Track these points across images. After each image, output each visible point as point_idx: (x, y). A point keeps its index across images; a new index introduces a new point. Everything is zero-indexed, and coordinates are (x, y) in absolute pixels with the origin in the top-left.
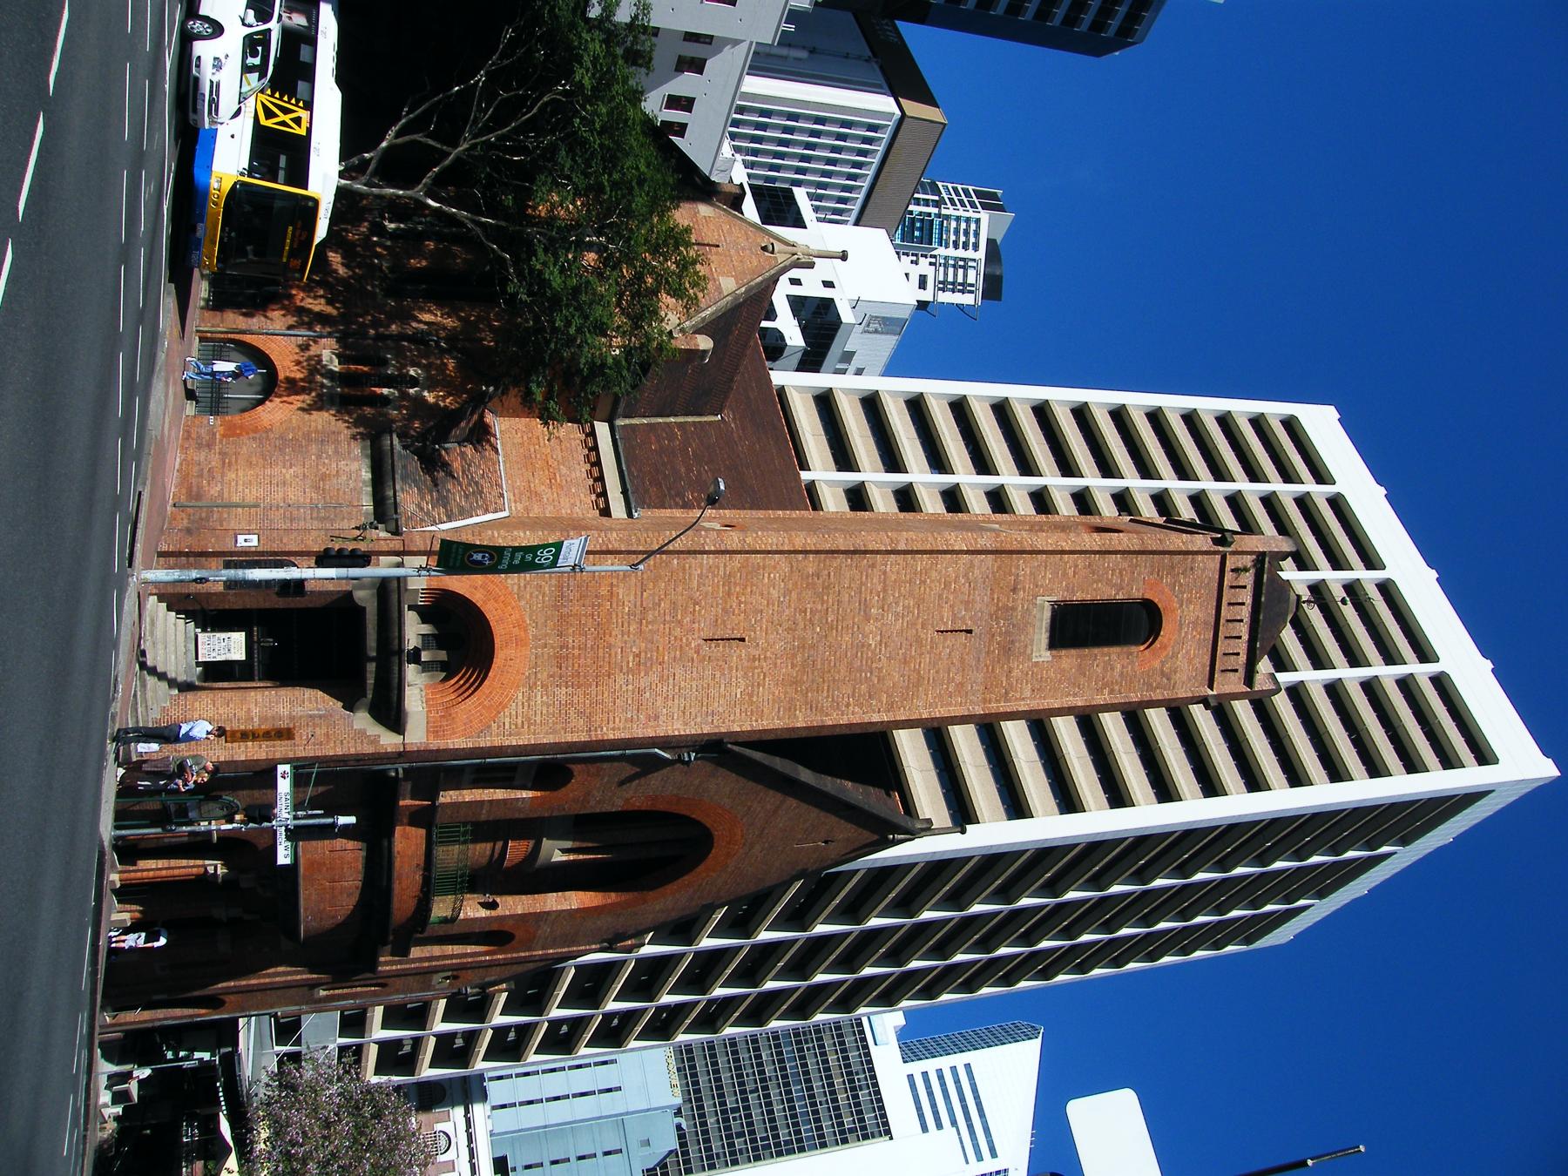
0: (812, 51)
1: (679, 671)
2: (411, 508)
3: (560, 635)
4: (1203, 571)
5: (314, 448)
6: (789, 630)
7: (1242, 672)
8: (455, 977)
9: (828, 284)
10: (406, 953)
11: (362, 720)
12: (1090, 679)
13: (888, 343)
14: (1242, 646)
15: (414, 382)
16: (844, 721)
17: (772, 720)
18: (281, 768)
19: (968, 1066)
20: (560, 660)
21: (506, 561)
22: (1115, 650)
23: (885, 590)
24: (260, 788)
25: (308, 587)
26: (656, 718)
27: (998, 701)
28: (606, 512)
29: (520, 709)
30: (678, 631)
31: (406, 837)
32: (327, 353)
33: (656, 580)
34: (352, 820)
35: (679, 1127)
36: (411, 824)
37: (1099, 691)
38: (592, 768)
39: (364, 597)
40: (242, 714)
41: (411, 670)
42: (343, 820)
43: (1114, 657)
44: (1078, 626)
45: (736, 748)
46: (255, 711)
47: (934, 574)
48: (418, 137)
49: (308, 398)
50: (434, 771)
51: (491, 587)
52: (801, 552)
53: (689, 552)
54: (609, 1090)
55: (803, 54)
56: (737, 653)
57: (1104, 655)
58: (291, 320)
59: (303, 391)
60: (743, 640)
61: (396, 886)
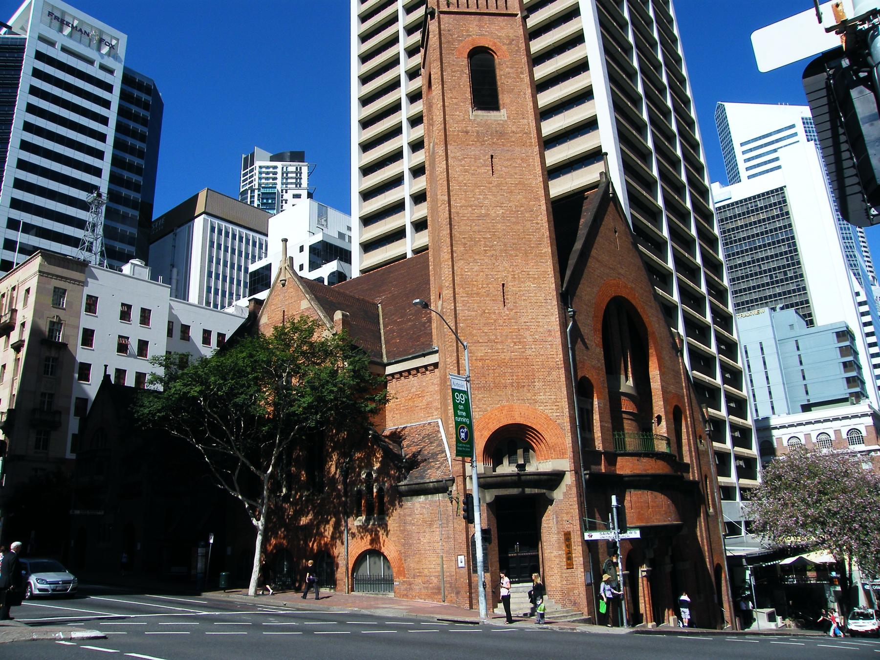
0: (173, 266)
1: (523, 320)
2: (438, 472)
3: (506, 387)
4: (449, 24)
5: (409, 528)
8: (700, 437)
9: (302, 249)
10: (687, 465)
11: (558, 494)
13: (333, 214)
15: (369, 475)
16: (546, 225)
17: (548, 266)
18: (587, 538)
19: (742, 145)
20: (520, 386)
21: (464, 420)
22: (498, 72)
23: (471, 206)
24: (597, 549)
25: (485, 527)
26: (550, 331)
27: (531, 138)
28: (436, 365)
29: (548, 408)
31: (622, 468)
32: (356, 522)
33: (473, 335)
34: (614, 498)
35: (782, 308)
36: (615, 465)
37: (522, 80)
38: (579, 365)
39: (490, 496)
41: (530, 469)
42: (614, 502)
43: (502, 73)
44: (485, 94)
45: (565, 285)
46: (555, 553)
47: (461, 179)
48: (235, 478)
49: (381, 532)
50: (585, 454)
51: (481, 427)
52: (452, 255)
53: (456, 317)
54: (762, 349)
55: (175, 271)
56: (511, 287)
57: (501, 78)
58: (338, 542)
59: (377, 535)
60: (503, 285)
61: (650, 472)
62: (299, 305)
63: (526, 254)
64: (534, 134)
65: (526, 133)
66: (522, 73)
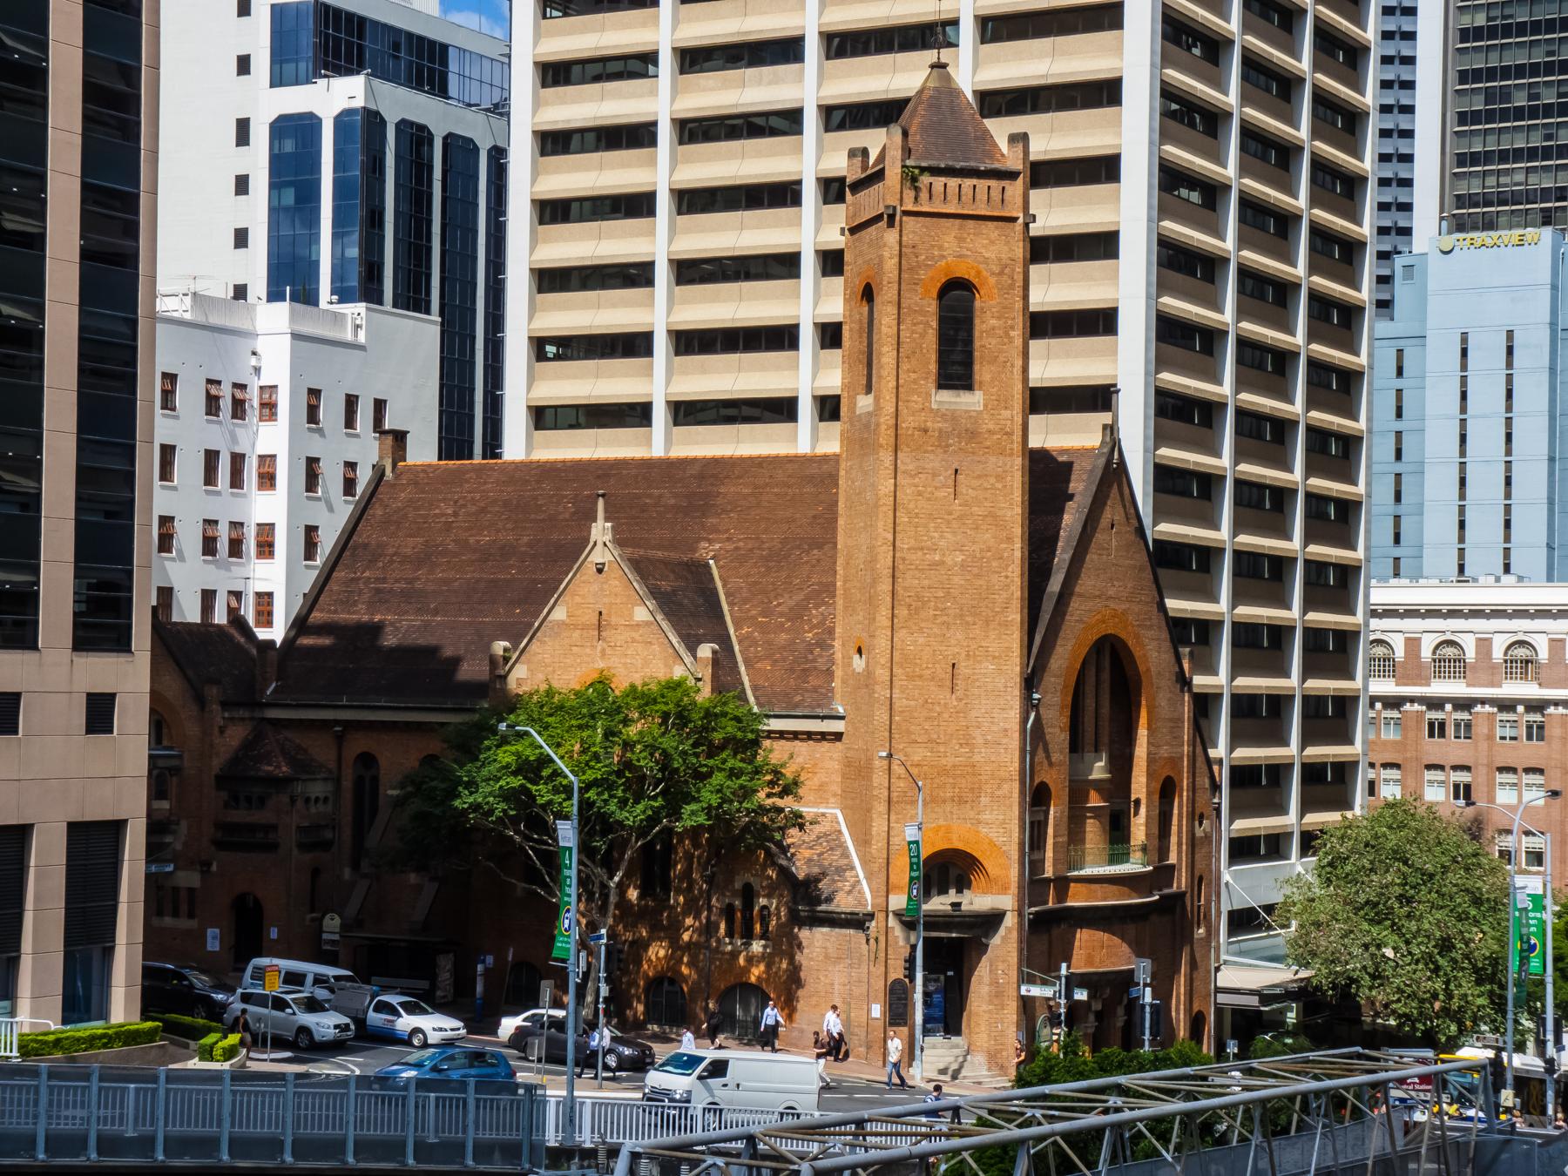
3: (944, 801)
6: (947, 625)
7: (1005, 183)
8: (1201, 817)
11: (996, 941)
12: (1001, 351)
14: (983, 184)
16: (1018, 581)
17: (1014, 639)
18: (1023, 992)
20: (961, 801)
22: (980, 327)
28: (838, 736)
29: (995, 831)
30: (946, 716)
33: (909, 732)
38: (1037, 768)
40: (986, 1016)
44: (956, 368)
46: (984, 1007)
47: (912, 506)
50: (1033, 885)
54: (1510, 351)
56: (963, 669)
62: (631, 615)
63: (987, 622)
64: (1017, 437)
65: (1007, 434)
66: (1012, 328)
